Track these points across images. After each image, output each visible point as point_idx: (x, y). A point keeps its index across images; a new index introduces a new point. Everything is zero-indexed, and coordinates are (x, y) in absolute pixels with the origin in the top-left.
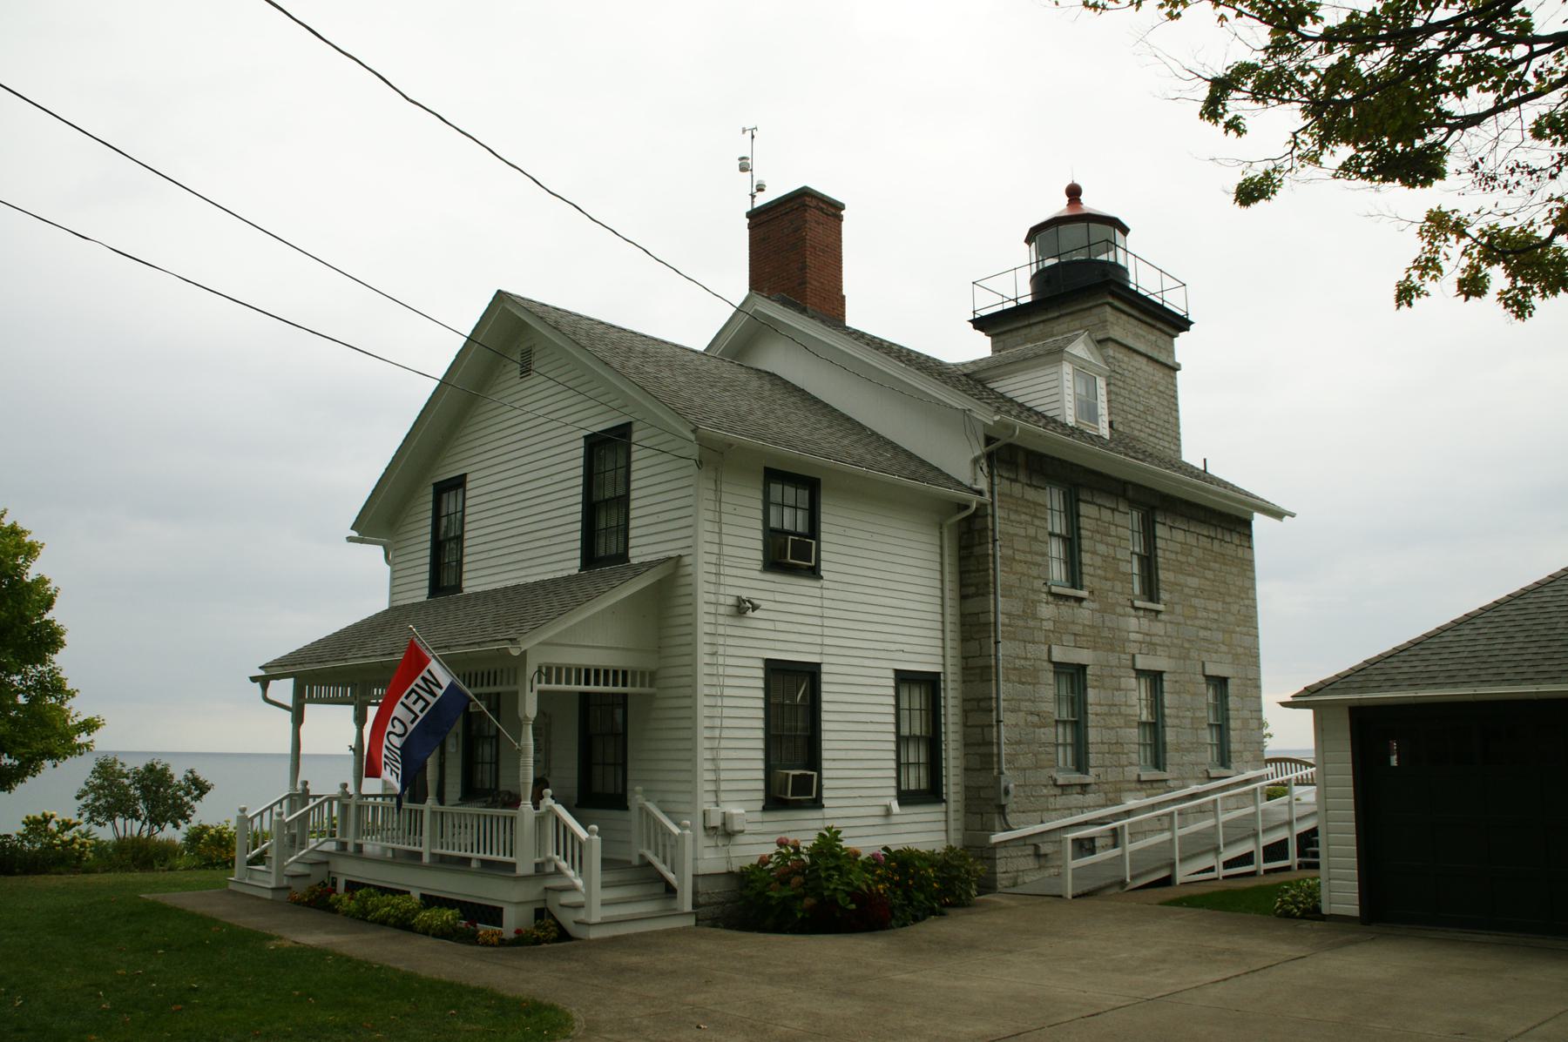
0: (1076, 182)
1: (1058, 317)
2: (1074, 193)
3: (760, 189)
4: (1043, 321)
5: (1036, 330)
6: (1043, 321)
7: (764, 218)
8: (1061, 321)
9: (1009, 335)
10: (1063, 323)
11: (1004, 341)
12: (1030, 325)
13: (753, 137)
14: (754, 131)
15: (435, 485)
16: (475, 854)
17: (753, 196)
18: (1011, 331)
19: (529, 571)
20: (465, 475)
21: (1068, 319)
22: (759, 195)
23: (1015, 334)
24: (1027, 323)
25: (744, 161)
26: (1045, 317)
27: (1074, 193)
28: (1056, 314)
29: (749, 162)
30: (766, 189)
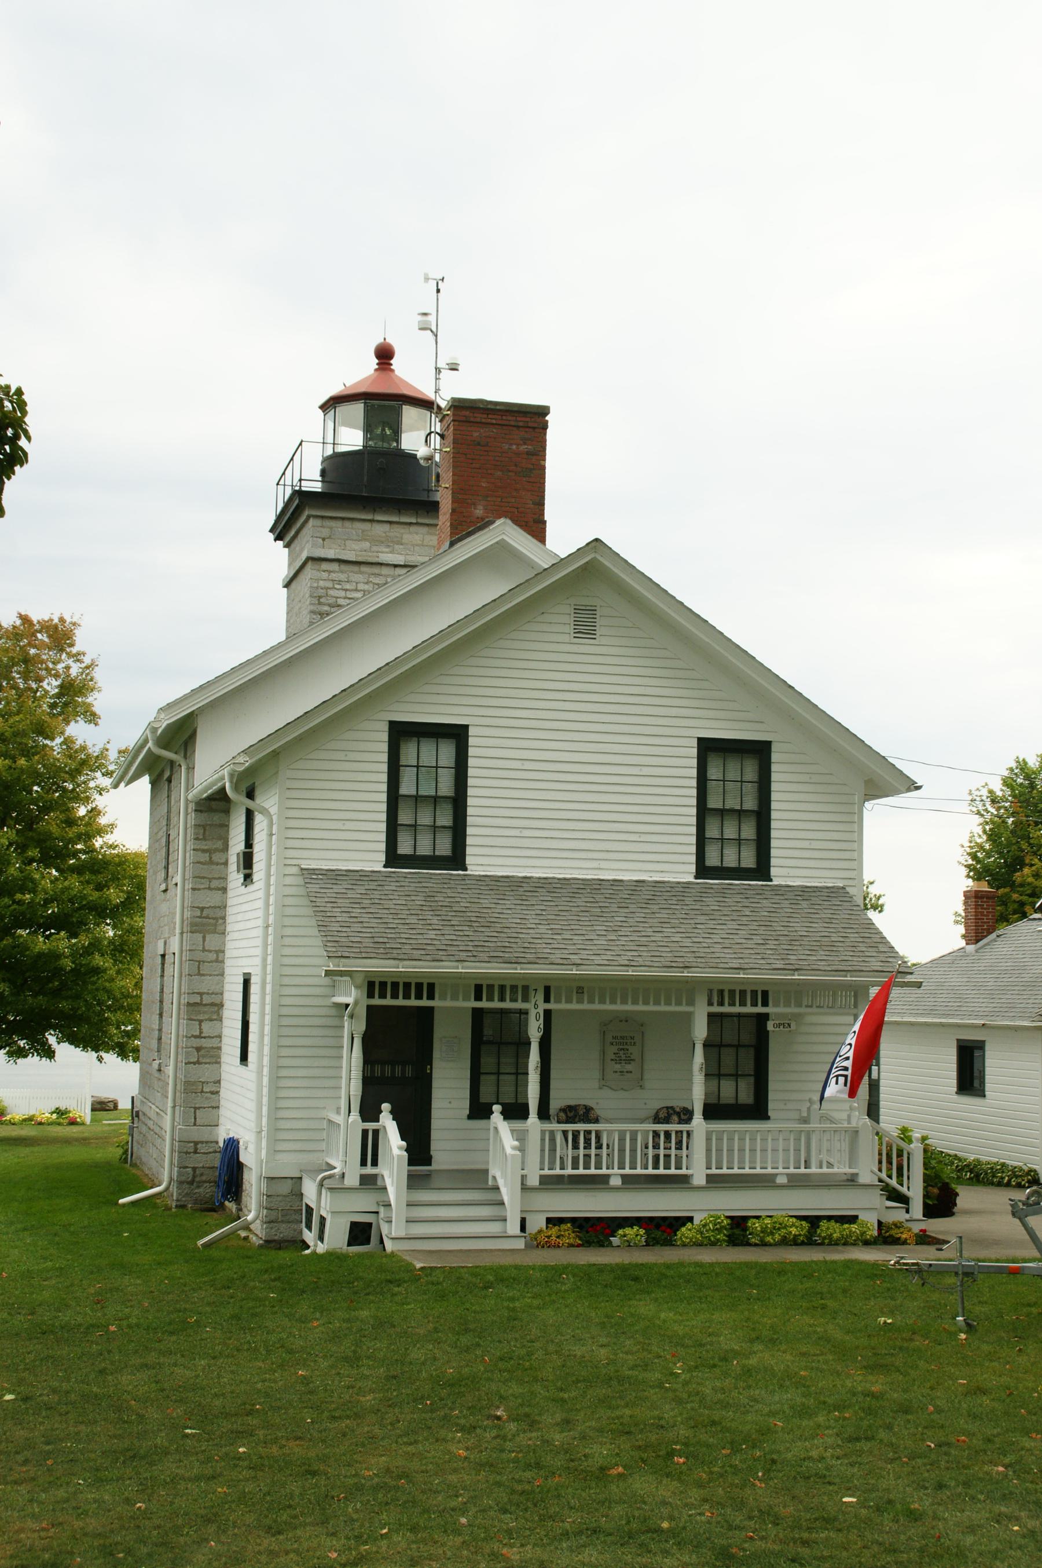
0: (389, 340)
1: (411, 524)
2: (384, 355)
3: (454, 368)
4: (390, 523)
5: (379, 530)
6: (390, 523)
7: (480, 417)
8: (413, 529)
9: (339, 523)
10: (417, 533)
11: (331, 528)
12: (371, 521)
13: (438, 291)
14: (440, 282)
15: (392, 724)
16: (781, 1170)
17: (438, 370)
18: (343, 519)
19: (603, 865)
20: (466, 727)
21: (425, 529)
22: (446, 374)
23: (347, 524)
24: (370, 517)
25: (424, 318)
26: (394, 518)
27: (384, 355)
28: (414, 521)
29: (432, 319)
30: (460, 368)
